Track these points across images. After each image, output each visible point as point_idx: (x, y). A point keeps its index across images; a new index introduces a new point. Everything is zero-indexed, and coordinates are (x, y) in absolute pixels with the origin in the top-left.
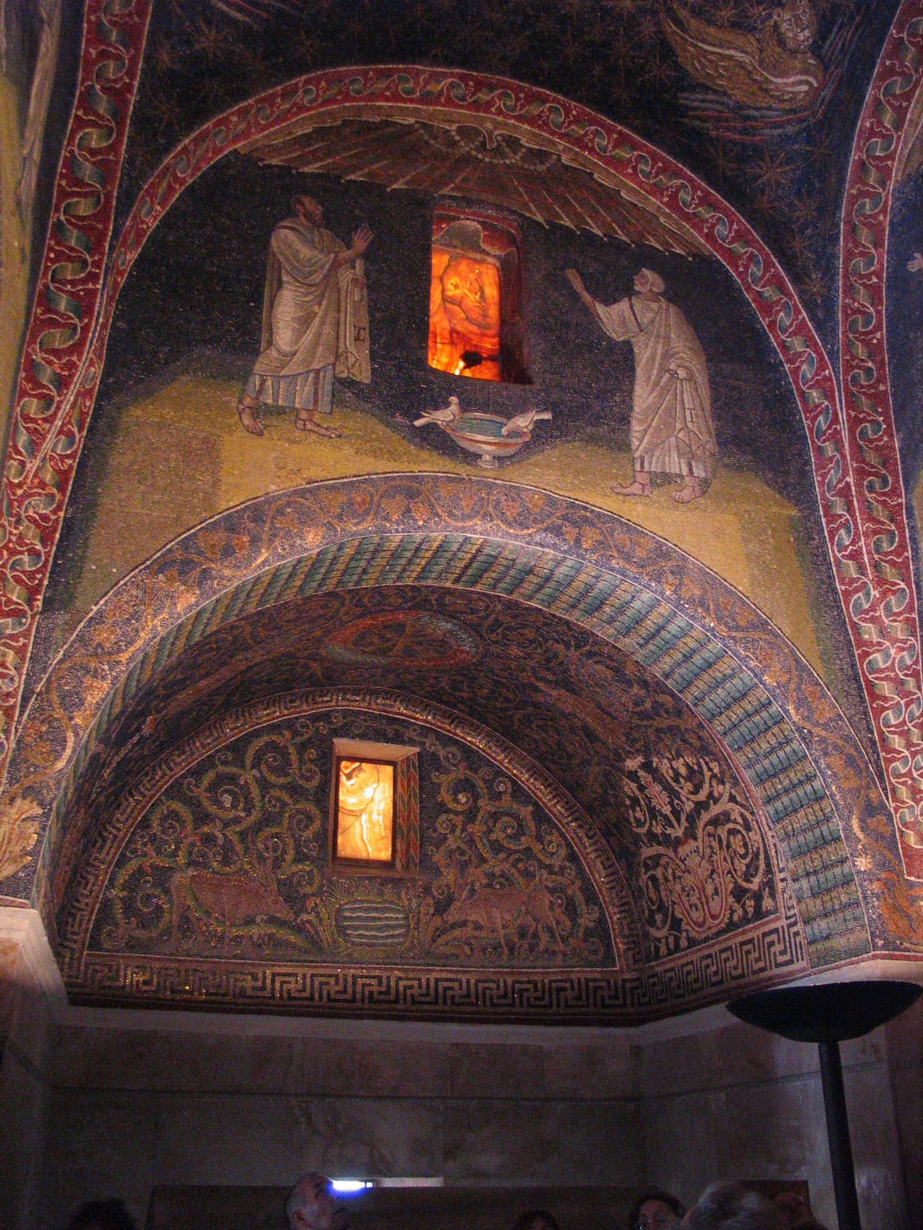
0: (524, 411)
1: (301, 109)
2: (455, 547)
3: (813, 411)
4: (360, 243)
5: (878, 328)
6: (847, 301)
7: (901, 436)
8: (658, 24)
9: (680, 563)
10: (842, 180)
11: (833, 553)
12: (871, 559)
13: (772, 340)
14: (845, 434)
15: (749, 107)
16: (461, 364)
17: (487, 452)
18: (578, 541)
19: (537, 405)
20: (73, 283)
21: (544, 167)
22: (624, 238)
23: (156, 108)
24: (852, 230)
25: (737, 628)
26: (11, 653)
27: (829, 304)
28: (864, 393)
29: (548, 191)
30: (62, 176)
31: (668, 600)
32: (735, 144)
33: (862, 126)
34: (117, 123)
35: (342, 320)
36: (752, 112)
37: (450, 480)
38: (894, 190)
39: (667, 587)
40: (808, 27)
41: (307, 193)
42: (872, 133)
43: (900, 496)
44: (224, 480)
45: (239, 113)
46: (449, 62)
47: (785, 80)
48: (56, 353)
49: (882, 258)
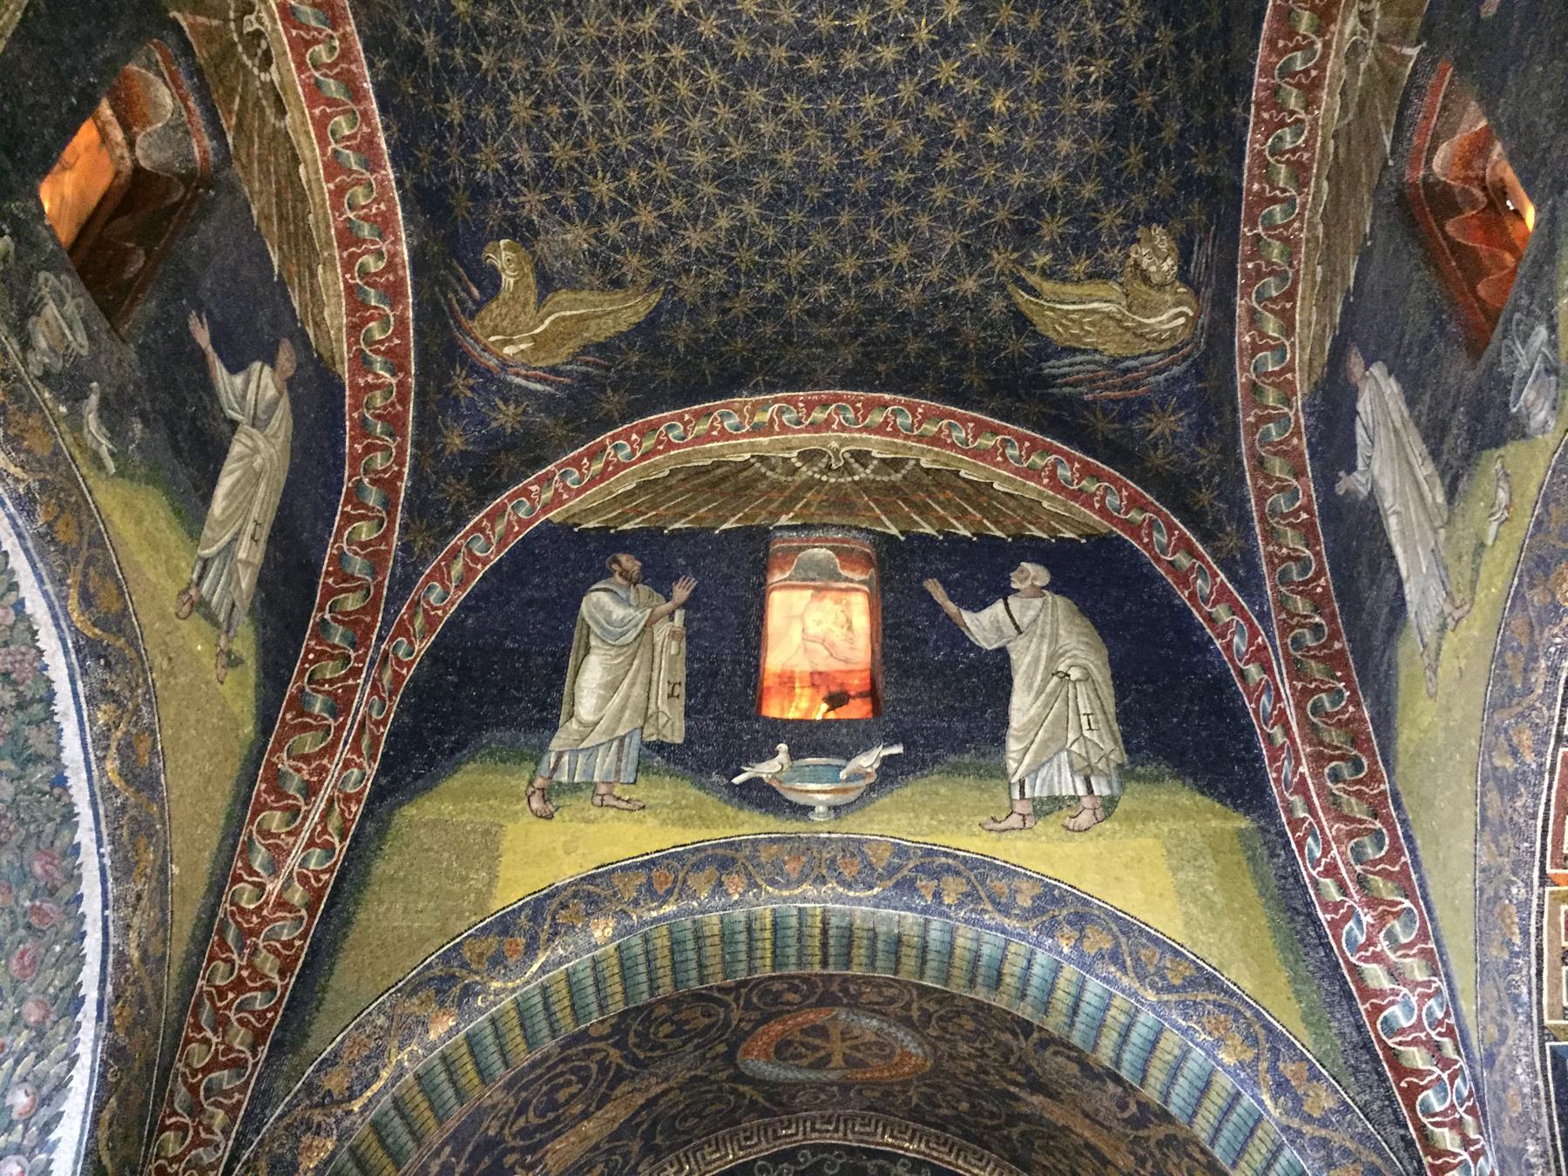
0: (867, 749)
1: (620, 466)
2: (794, 922)
3: (1255, 693)
4: (681, 592)
5: (1320, 573)
6: (1270, 548)
8: (1008, 297)
9: (1080, 909)
10: (1235, 410)
11: (1307, 872)
12: (1351, 871)
13: (1196, 614)
15: (1127, 358)
16: (825, 707)
17: (821, 803)
18: (937, 895)
19: (885, 738)
20: (331, 682)
21: (899, 476)
22: (999, 534)
23: (443, 491)
24: (1260, 463)
25: (1171, 989)
26: (220, 1114)
28: (1314, 657)
29: (905, 501)
30: (328, 574)
31: (1069, 959)
32: (1115, 401)
34: (388, 514)
35: (655, 678)
37: (772, 841)
38: (1303, 405)
39: (1063, 943)
41: (625, 550)
42: (1256, 348)
43: (1381, 781)
44: (502, 874)
45: (538, 481)
46: (771, 388)
48: (306, 759)
49: (1307, 488)
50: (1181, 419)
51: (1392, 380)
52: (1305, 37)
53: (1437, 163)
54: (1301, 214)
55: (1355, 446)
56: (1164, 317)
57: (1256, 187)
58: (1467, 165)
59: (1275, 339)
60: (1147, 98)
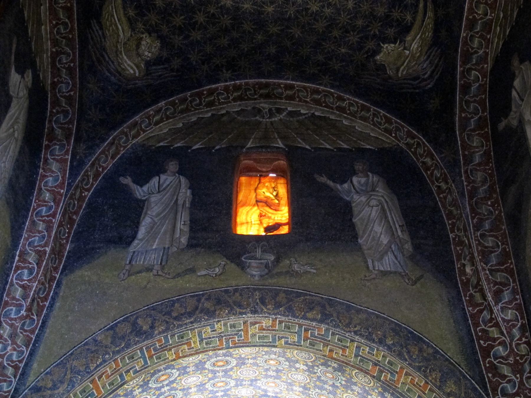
7: (73, 246)
10: (125, 122)
11: (13, 277)
13: (43, 153)
14: (55, 226)
15: (107, 54)
24: (112, 143)
27: (81, 164)
33: (149, 111)
36: (106, 56)
38: (134, 144)
40: (152, 53)
43: (57, 273)
47: (127, 60)
49: (110, 164)
50: (98, 92)
51: (189, 192)
52: (259, 93)
53: (246, 161)
54: (196, 109)
55: (147, 182)
56: (129, 62)
57: (205, 92)
58: (244, 169)
59: (153, 122)
60: (201, 18)
